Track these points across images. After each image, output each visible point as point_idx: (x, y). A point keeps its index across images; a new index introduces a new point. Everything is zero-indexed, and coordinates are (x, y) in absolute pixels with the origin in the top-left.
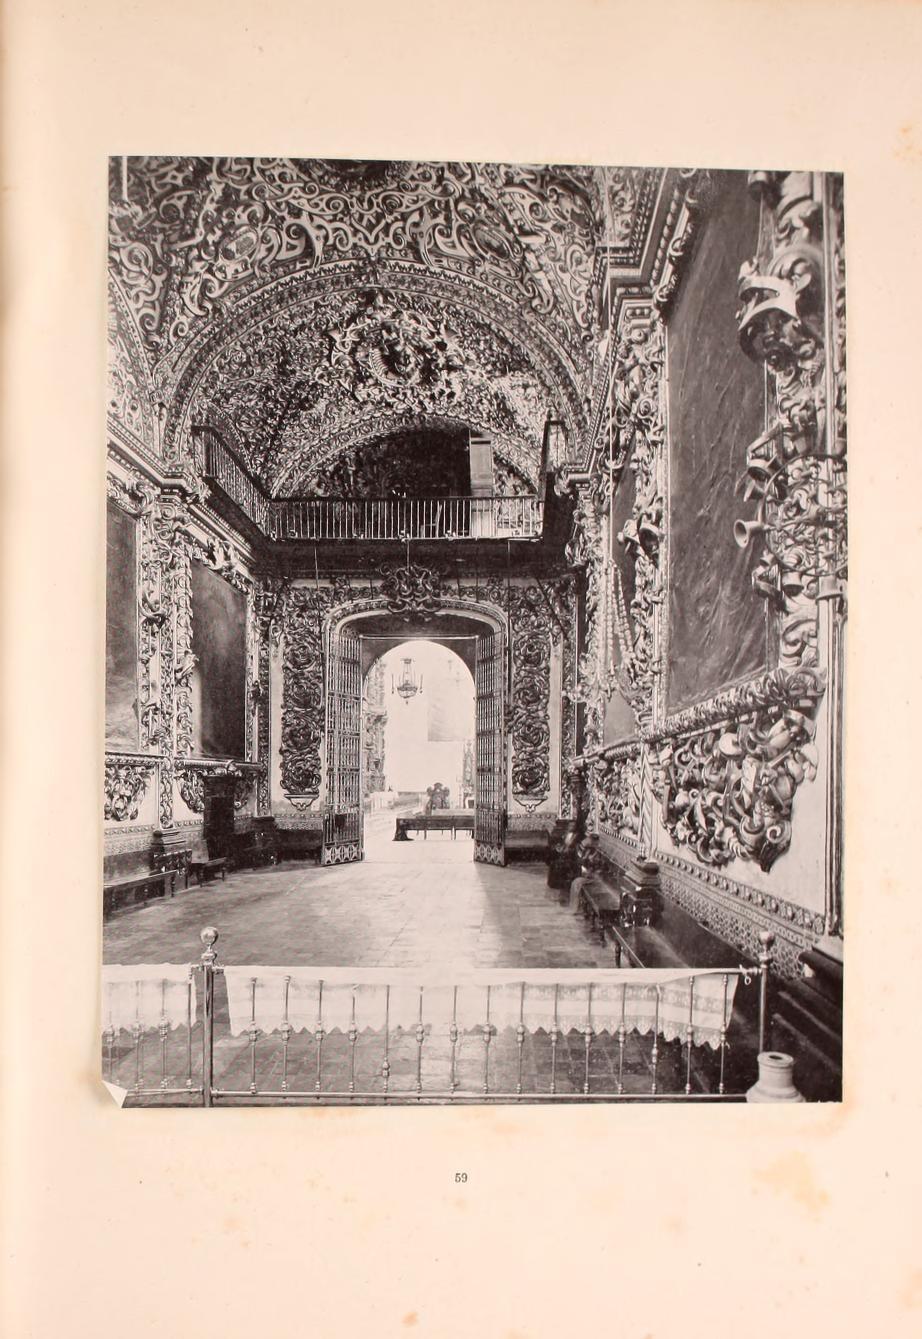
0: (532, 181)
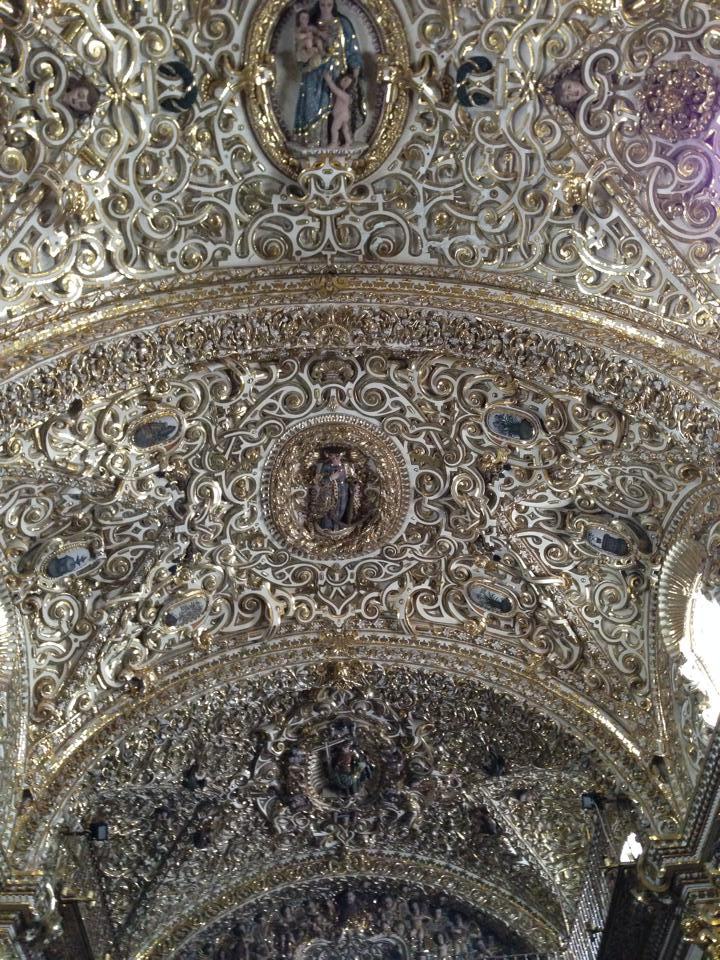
0: (547, 523)
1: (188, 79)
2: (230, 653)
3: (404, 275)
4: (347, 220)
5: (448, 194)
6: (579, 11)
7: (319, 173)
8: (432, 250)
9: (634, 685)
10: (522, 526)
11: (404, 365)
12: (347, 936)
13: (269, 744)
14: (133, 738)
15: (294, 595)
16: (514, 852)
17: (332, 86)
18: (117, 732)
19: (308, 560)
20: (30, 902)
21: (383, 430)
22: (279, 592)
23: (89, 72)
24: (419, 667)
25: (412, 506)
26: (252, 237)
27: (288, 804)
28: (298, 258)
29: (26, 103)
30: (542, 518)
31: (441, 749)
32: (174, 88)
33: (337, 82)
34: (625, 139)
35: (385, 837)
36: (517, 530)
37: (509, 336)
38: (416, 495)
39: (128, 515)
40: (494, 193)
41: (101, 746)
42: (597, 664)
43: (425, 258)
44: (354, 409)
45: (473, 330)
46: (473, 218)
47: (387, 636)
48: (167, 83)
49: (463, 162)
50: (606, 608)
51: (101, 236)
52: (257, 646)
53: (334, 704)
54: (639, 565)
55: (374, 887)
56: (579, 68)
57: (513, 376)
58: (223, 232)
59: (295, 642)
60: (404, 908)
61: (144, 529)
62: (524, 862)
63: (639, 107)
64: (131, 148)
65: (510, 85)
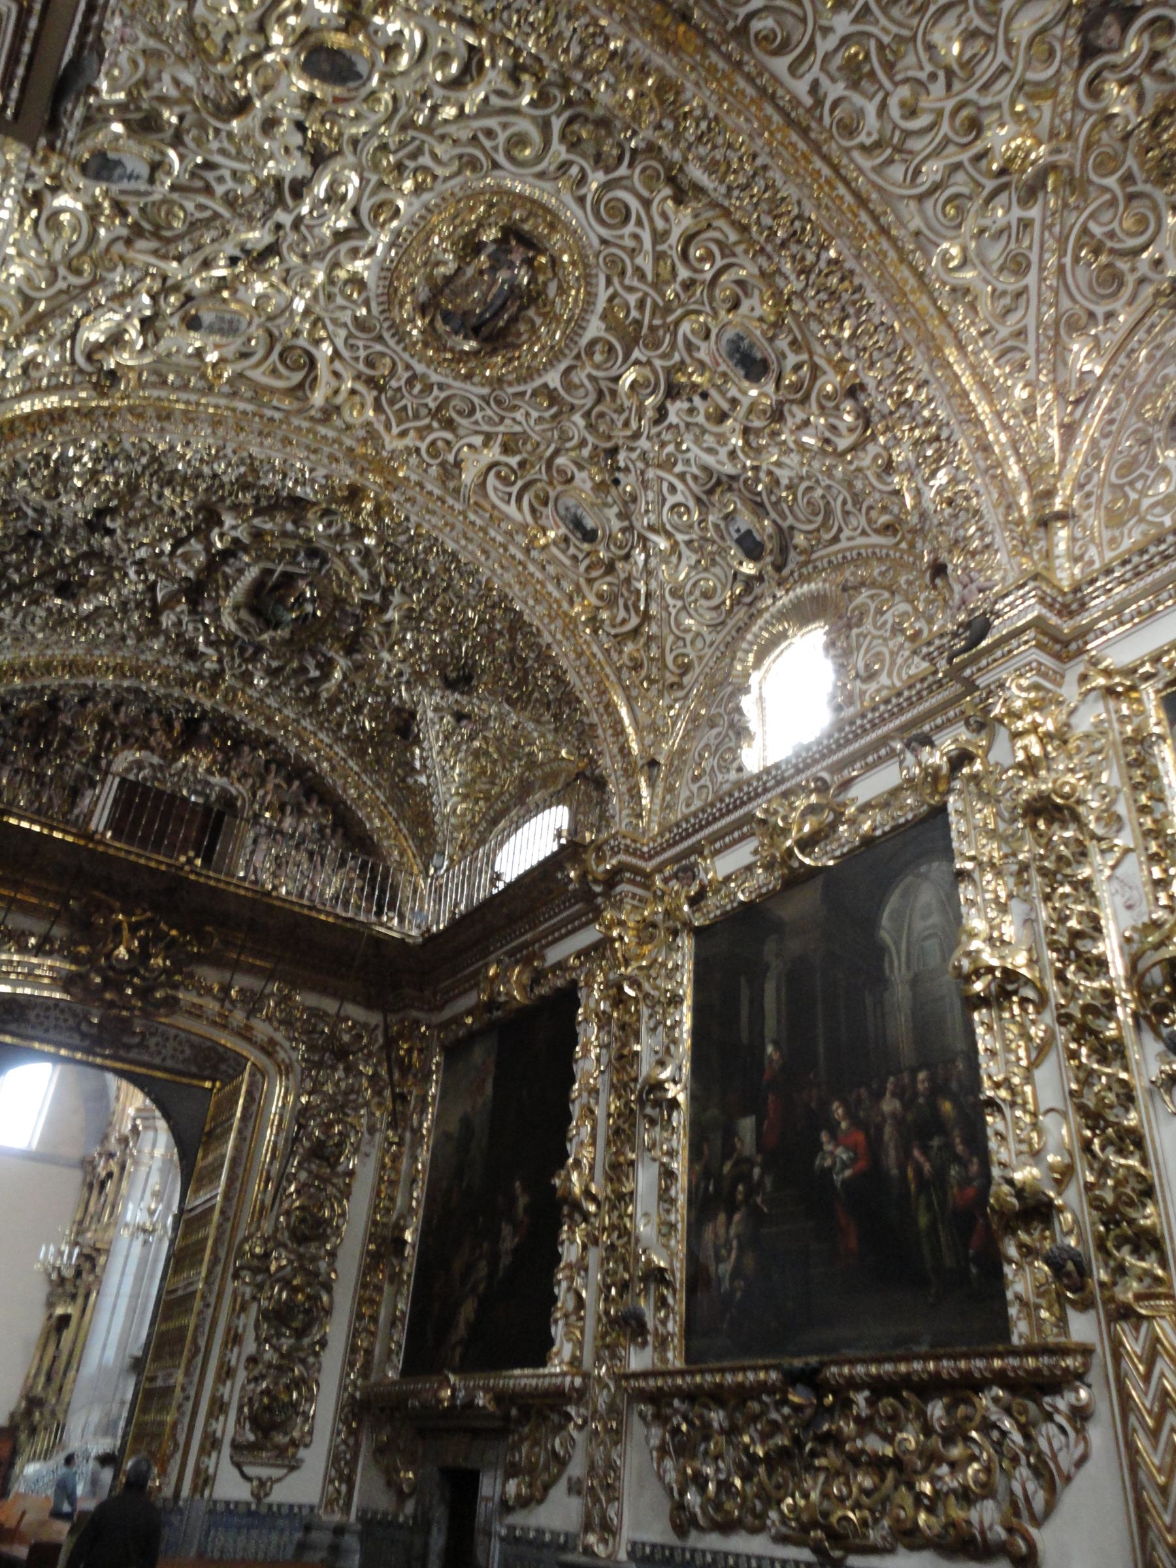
0: (695, 478)
2: (241, 406)
3: (762, 91)
5: (885, 30)
8: (815, 87)
9: (672, 685)
12: (185, 765)
14: (82, 446)
16: (418, 765)
21: (597, 255)
22: (338, 366)
25: (562, 366)
30: (695, 470)
36: (659, 466)
37: (830, 262)
38: (578, 357)
40: (933, 77)
42: (647, 646)
43: (801, 87)
44: (583, 207)
45: (797, 224)
47: (437, 492)
52: (277, 416)
53: (320, 528)
54: (760, 578)
56: (1135, 11)
57: (789, 302)
59: (325, 437)
61: (230, 184)
62: (423, 780)
63: (1149, 109)
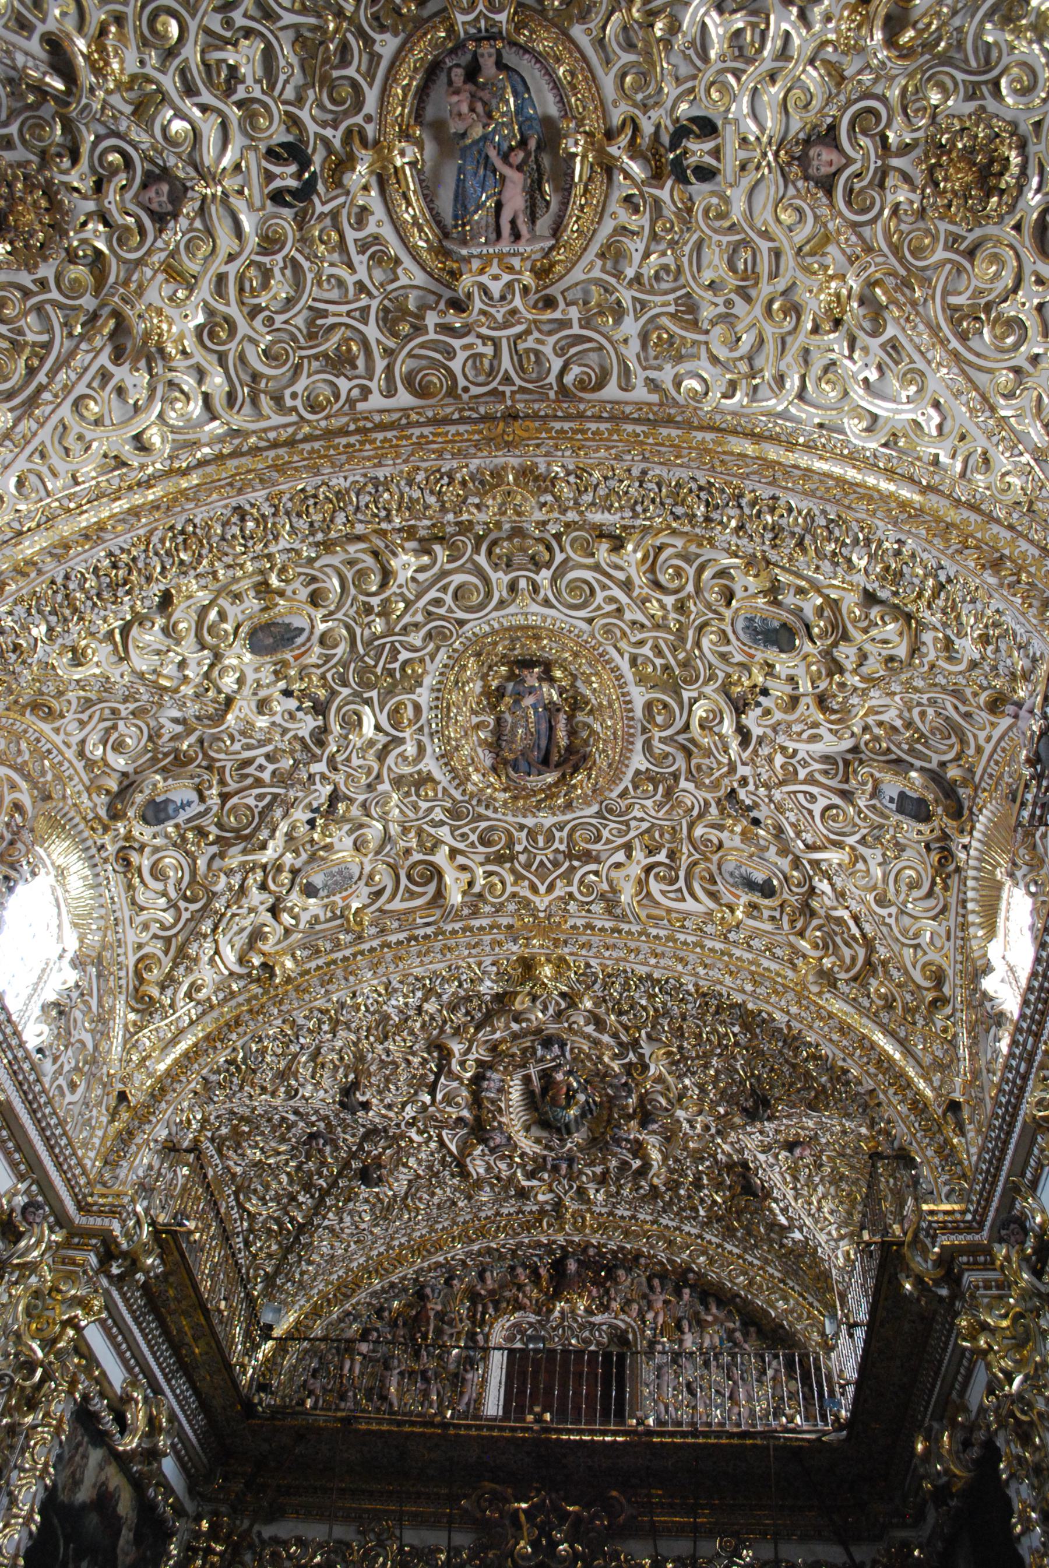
0: (826, 772)
1: (304, 162)
3: (612, 418)
4: (530, 343)
6: (830, 49)
7: (484, 279)
9: (934, 1003)
10: (791, 777)
11: (618, 545)
12: (562, 1312)
13: (454, 1062)
15: (482, 864)
16: (783, 1221)
17: (498, 163)
18: (241, 1030)
19: (499, 816)
20: (116, 1227)
21: (594, 637)
23: (172, 161)
24: (647, 969)
25: (639, 745)
26: (401, 368)
27: (483, 1141)
28: (465, 397)
29: (91, 206)
31: (687, 1082)
32: (286, 176)
33: (505, 158)
34: (903, 227)
35: (618, 1193)
36: (781, 783)
37: (753, 504)
38: (644, 730)
39: (248, 747)
41: (219, 1045)
42: (886, 972)
43: (641, 393)
44: (553, 607)
45: (703, 495)
46: (702, 338)
47: (608, 925)
48: (276, 170)
49: (685, 260)
50: (902, 897)
51: (195, 373)
52: (429, 930)
55: (603, 1256)
56: (833, 128)
58: (360, 362)
59: (481, 928)
60: (640, 1284)
61: (271, 767)
62: (797, 1235)
64: (231, 258)
65: (743, 155)
